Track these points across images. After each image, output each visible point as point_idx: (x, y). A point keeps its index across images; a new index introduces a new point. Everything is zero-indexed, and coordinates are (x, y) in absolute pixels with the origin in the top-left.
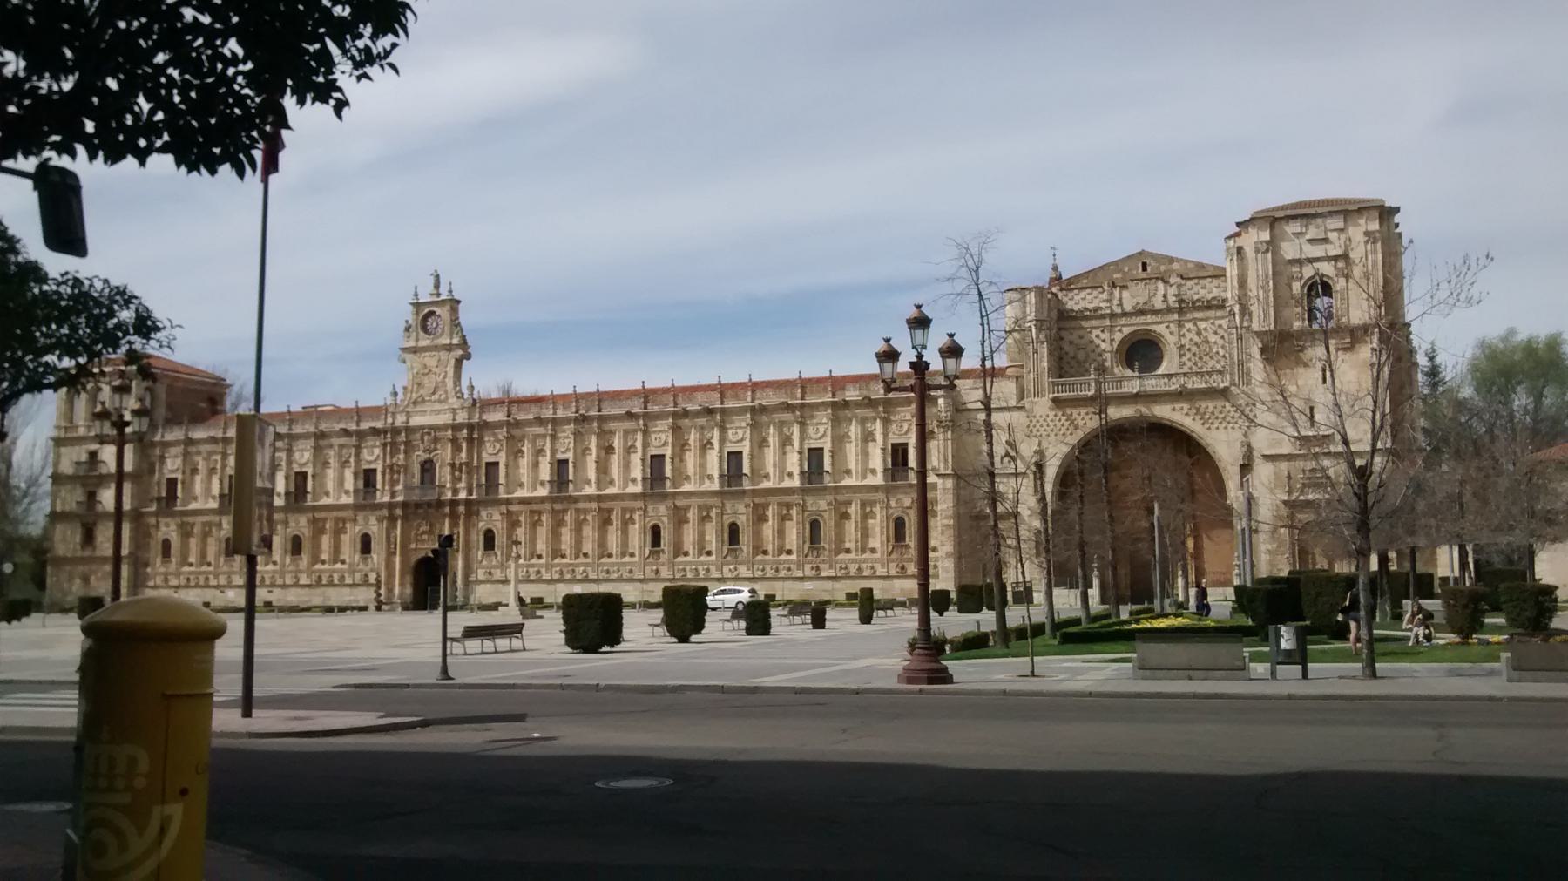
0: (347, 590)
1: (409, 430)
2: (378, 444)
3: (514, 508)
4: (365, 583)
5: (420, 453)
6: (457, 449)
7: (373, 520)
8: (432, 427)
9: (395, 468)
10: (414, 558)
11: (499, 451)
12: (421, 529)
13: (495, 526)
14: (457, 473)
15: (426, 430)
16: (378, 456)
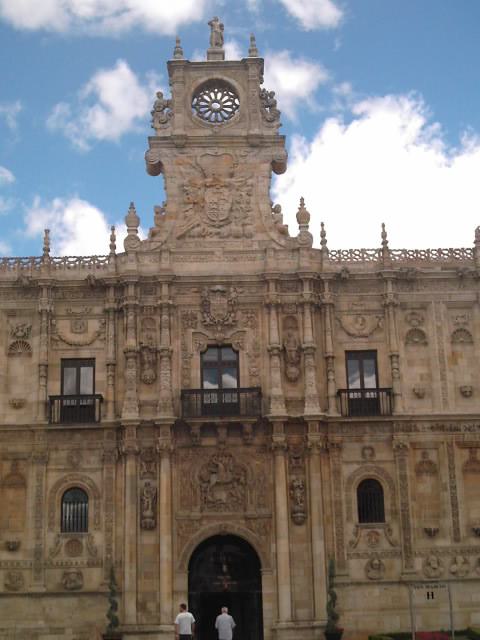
0: (25, 605)
1: (174, 281)
2: (98, 310)
3: (426, 437)
4: (71, 588)
5: (200, 329)
6: (290, 323)
7: (92, 461)
8: (229, 282)
9: (147, 356)
10: (196, 537)
11: (377, 328)
12: (214, 479)
13: (383, 471)
14: (293, 370)
15: (219, 287)
16: (99, 334)
